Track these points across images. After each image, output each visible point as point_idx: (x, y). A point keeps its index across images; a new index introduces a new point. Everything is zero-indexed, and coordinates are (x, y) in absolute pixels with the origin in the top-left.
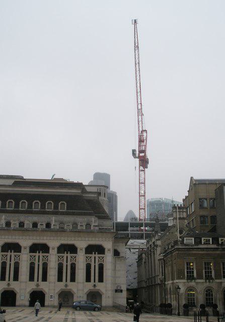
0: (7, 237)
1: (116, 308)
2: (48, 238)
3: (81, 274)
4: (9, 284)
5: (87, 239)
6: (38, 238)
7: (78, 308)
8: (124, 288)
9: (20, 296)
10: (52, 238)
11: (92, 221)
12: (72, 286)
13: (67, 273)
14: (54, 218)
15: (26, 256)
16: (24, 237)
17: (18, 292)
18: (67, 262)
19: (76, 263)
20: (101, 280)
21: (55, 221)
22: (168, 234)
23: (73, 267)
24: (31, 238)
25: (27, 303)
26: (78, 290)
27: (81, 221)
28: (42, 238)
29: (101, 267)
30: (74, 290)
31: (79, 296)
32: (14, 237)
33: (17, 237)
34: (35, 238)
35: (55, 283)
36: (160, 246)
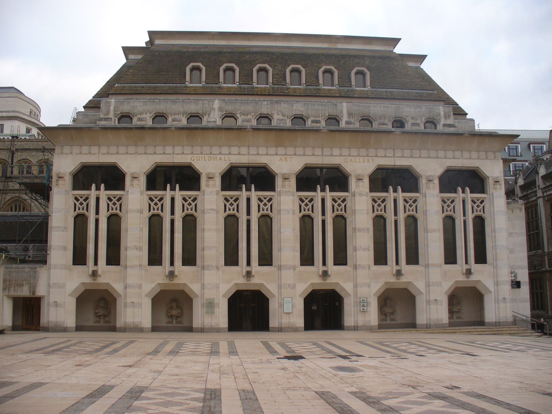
0: (235, 150)
2: (345, 152)
5: (441, 154)
6: (318, 151)
8: (524, 276)
9: (281, 305)
10: (354, 152)
11: (439, 115)
12: (413, 276)
13: (397, 243)
14: (345, 104)
15: (291, 198)
16: (281, 150)
17: (276, 295)
19: (419, 216)
20: (481, 257)
21: (350, 114)
24: (300, 151)
25: (300, 322)
26: (428, 285)
28: (327, 151)
29: (480, 224)
30: (420, 285)
31: (432, 298)
32: (253, 150)
33: (262, 150)
34: (309, 151)
35: (369, 268)
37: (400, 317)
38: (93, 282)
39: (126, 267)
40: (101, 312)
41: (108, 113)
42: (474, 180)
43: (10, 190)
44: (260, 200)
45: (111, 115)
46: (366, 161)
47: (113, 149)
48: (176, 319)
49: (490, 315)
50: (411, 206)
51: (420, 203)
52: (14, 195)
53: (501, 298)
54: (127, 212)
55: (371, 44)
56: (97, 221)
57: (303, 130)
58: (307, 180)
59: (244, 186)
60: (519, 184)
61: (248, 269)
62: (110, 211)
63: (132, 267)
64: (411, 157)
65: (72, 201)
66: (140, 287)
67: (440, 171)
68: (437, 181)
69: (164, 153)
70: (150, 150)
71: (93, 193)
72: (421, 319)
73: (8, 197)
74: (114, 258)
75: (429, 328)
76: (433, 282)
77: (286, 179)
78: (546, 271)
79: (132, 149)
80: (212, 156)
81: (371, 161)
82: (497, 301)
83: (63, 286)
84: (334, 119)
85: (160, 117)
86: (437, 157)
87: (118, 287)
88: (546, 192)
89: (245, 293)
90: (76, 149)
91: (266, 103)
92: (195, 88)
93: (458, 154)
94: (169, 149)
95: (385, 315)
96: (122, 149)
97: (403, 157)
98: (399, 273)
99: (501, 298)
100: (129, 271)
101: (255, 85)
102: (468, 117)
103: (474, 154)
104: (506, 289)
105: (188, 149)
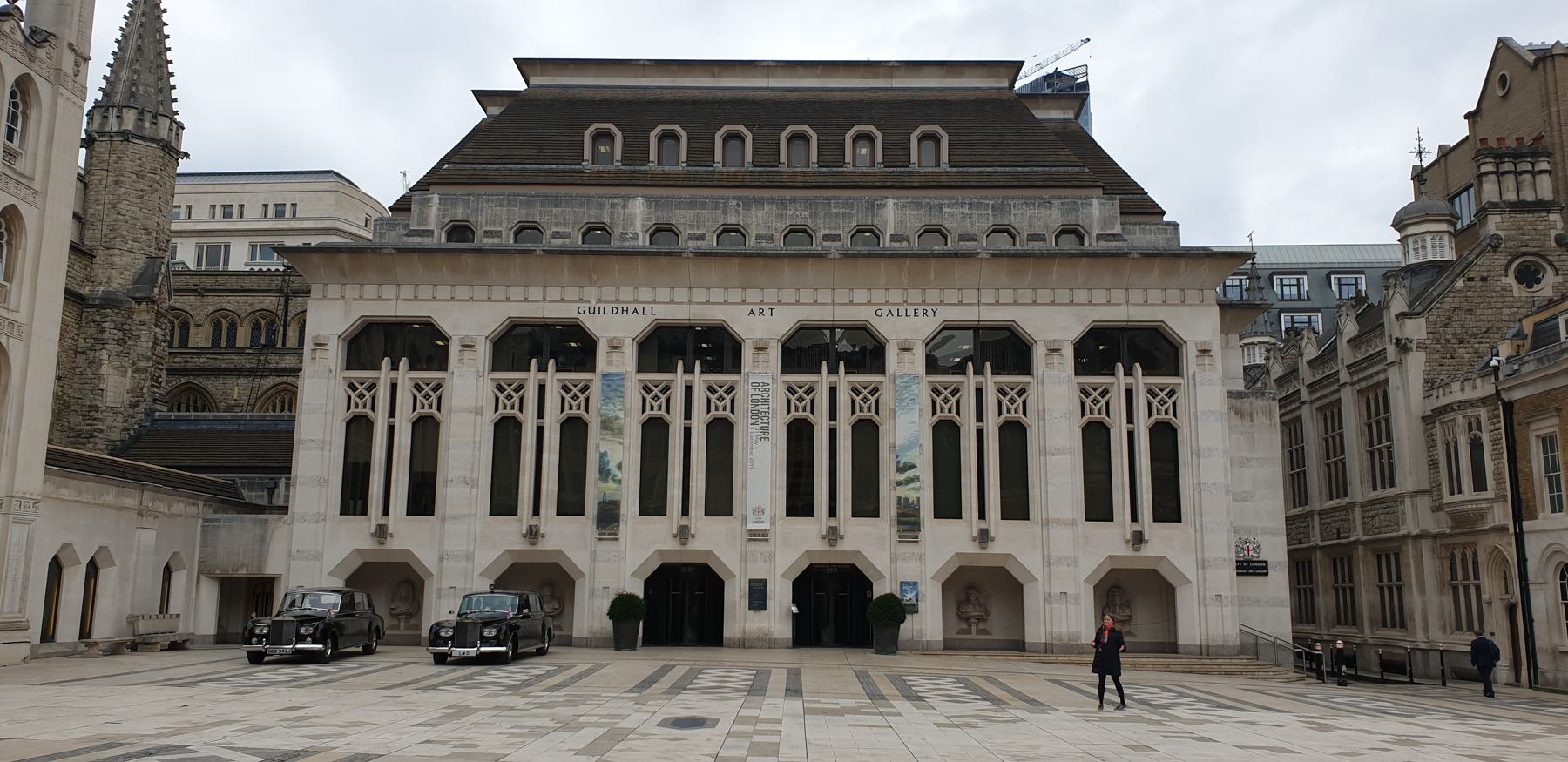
0: (663, 294)
1: (1249, 655)
2: (879, 296)
3: (1057, 473)
4: (684, 534)
5: (1081, 295)
6: (825, 296)
7: (1042, 648)
8: (1275, 550)
10: (896, 296)
11: (1089, 216)
12: (1012, 542)
18: (980, 418)
19: (1031, 422)
20: (1168, 508)
22: (1460, 283)
23: (1014, 436)
25: (784, 630)
26: (1047, 562)
27: (1037, 217)
28: (842, 295)
29: (1165, 438)
31: (1056, 590)
32: (699, 295)
33: (717, 295)
34: (807, 296)
36: (1421, 346)
37: (997, 628)
38: (376, 547)
39: (444, 519)
40: (402, 607)
41: (423, 219)
42: (1154, 350)
43: (271, 370)
44: (712, 390)
45: (432, 225)
46: (920, 313)
47: (425, 291)
48: (407, 620)
49: (1189, 631)
50: (946, 400)
51: (1032, 397)
52: (278, 380)
53: (1211, 594)
54: (450, 411)
55: (960, 75)
56: (391, 428)
57: (739, 255)
58: (803, 351)
59: (680, 363)
60: (1306, 358)
61: (684, 521)
62: (419, 409)
63: (455, 518)
64: (1016, 303)
65: (341, 391)
66: (469, 557)
67: (1077, 331)
68: (1068, 352)
69: (526, 300)
70: (498, 292)
71: (384, 374)
72: (1035, 633)
73: (268, 382)
74: (422, 499)
75: (1052, 651)
76: (1061, 558)
77: (760, 349)
78: (1357, 542)
79: (462, 291)
80: (619, 306)
81: (930, 313)
82: (1203, 602)
83: (317, 556)
84: (868, 231)
85: (525, 229)
86: (1072, 303)
87: (426, 557)
88: (1357, 372)
89: (683, 570)
90: (351, 291)
91: (734, 203)
92: (599, 174)
93: (1118, 295)
94: (535, 292)
95: (967, 620)
96: (444, 291)
97: (997, 303)
98: (984, 536)
99: (1211, 594)
100: (448, 525)
101: (718, 166)
102: (1166, 218)
103: (1155, 295)
104: (1224, 577)
105: (572, 293)
